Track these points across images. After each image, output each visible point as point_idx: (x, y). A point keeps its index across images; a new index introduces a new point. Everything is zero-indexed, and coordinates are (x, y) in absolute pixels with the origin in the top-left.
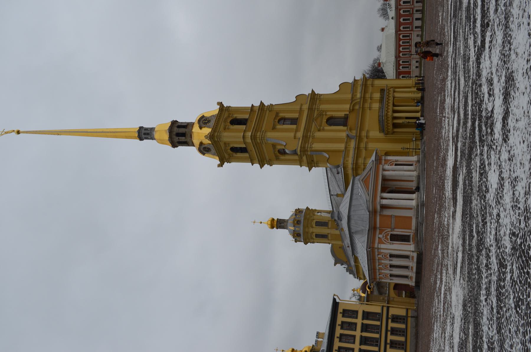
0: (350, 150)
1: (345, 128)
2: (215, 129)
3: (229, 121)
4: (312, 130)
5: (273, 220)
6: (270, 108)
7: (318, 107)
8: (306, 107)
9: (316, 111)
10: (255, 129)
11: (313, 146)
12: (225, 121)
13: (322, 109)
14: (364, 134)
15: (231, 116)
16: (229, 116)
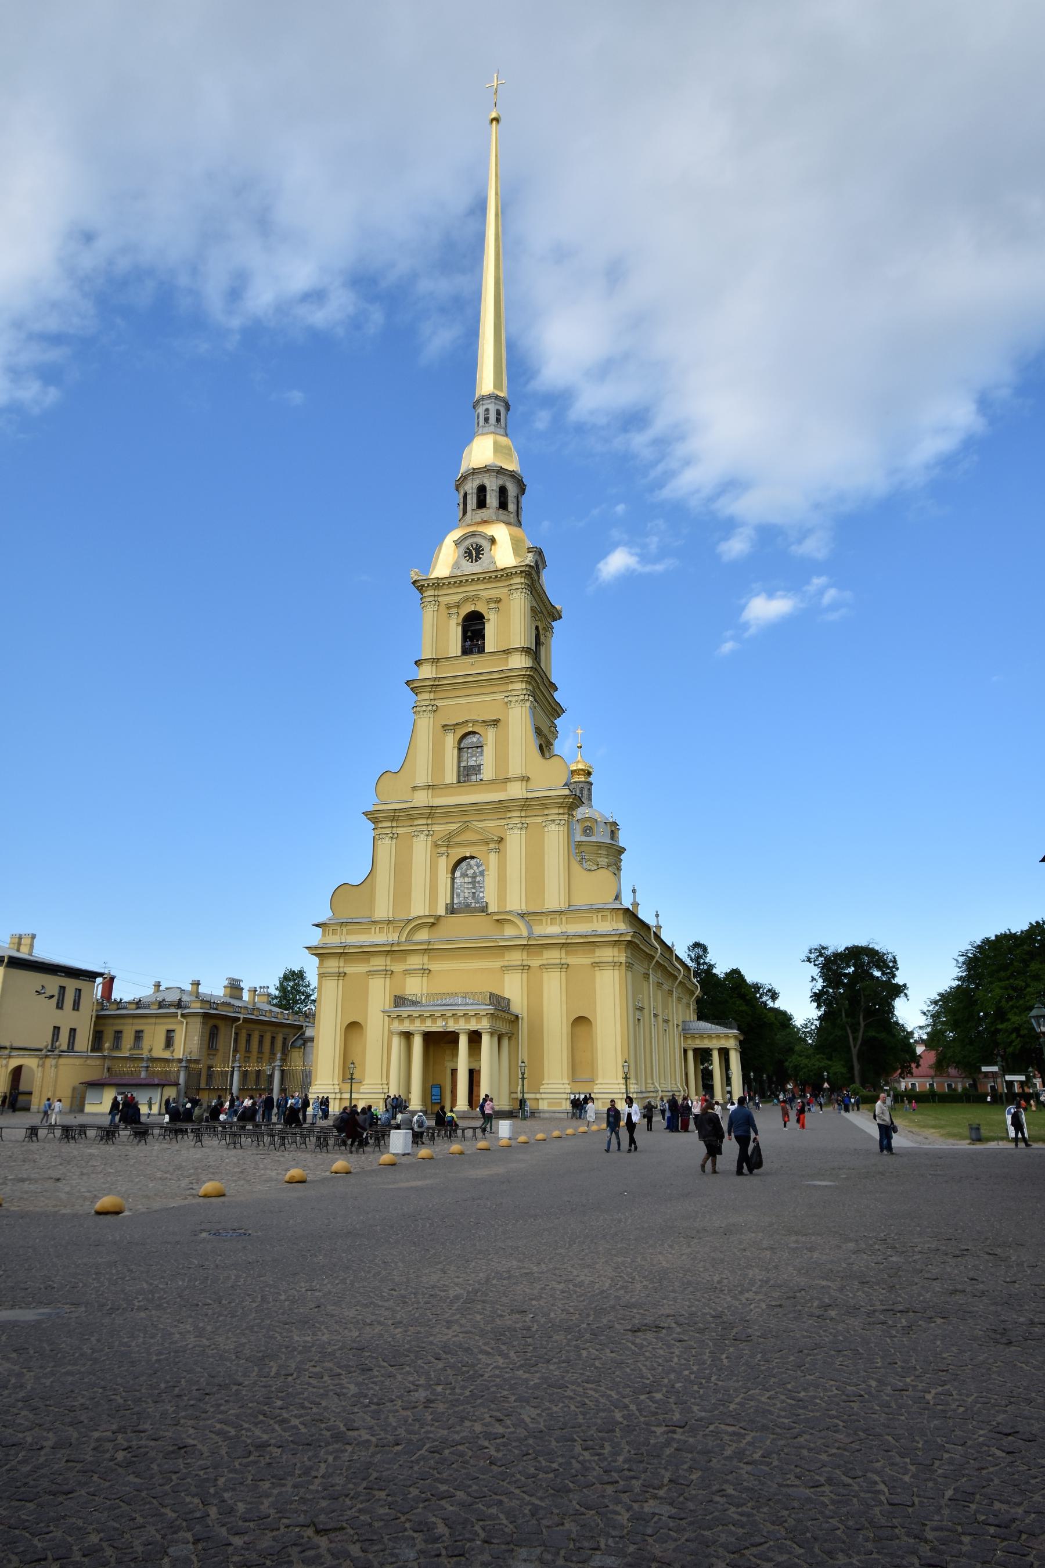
0: (370, 933)
1: (441, 911)
2: (444, 584)
3: (473, 608)
4: (436, 828)
5: (589, 774)
6: (509, 698)
7: (510, 826)
8: (516, 791)
9: (503, 822)
10: (436, 683)
11: (387, 841)
12: (475, 598)
13: (508, 837)
14: (415, 962)
15: (492, 605)
16: (489, 601)
